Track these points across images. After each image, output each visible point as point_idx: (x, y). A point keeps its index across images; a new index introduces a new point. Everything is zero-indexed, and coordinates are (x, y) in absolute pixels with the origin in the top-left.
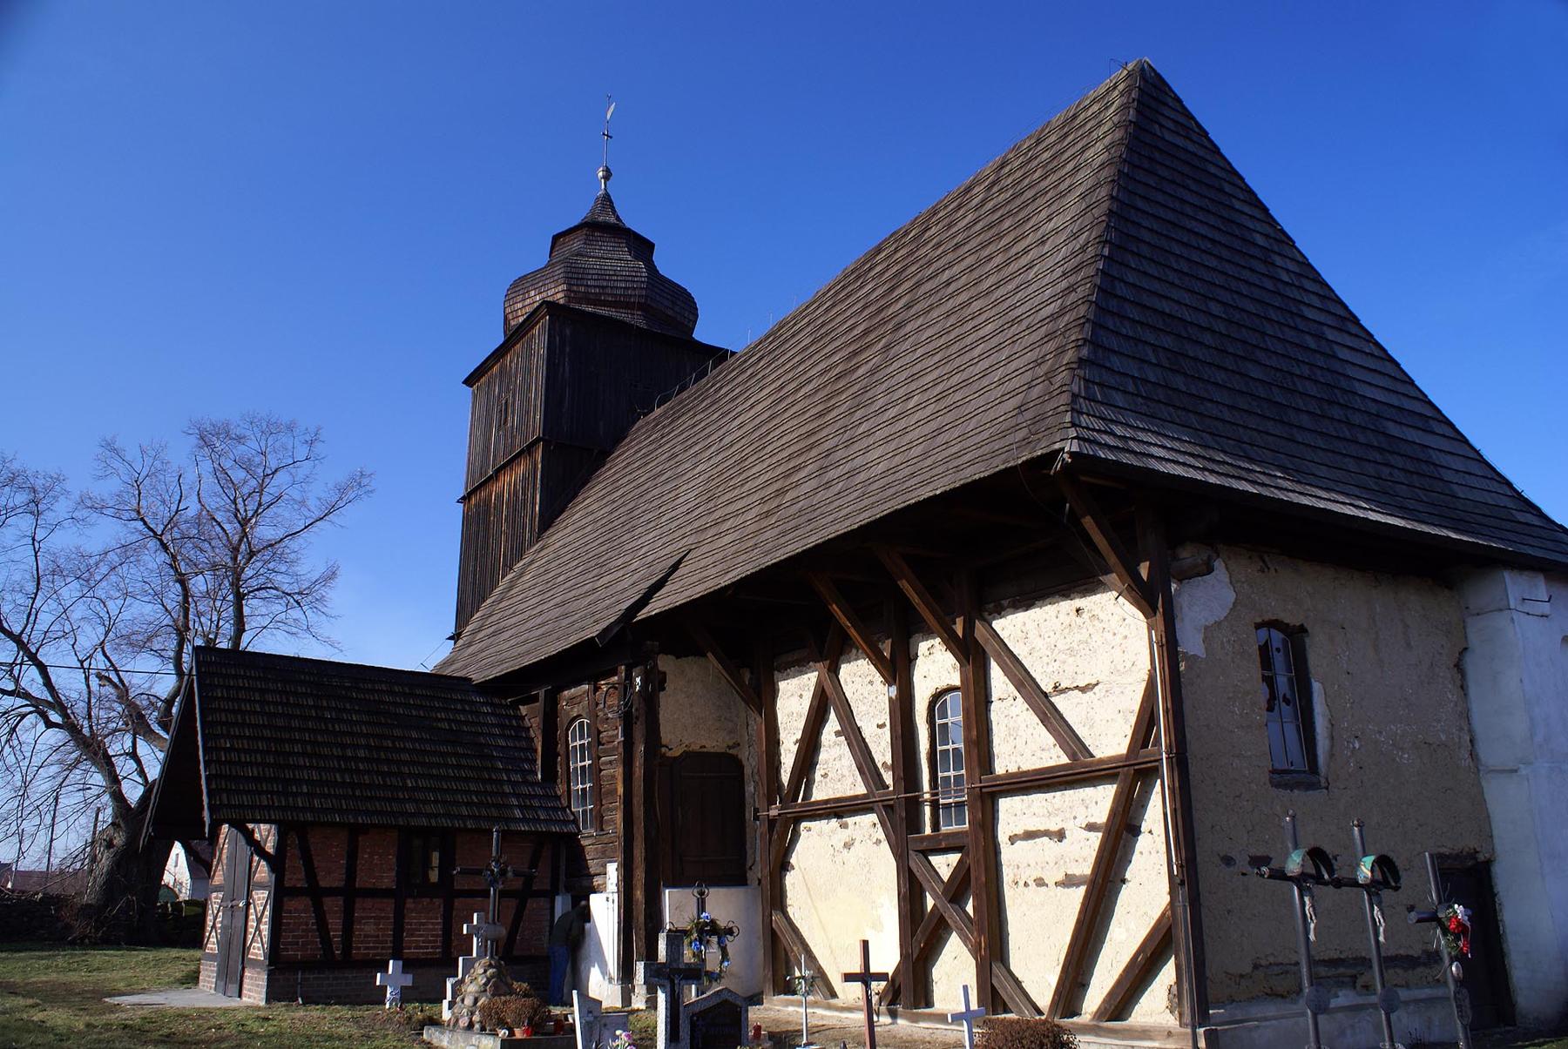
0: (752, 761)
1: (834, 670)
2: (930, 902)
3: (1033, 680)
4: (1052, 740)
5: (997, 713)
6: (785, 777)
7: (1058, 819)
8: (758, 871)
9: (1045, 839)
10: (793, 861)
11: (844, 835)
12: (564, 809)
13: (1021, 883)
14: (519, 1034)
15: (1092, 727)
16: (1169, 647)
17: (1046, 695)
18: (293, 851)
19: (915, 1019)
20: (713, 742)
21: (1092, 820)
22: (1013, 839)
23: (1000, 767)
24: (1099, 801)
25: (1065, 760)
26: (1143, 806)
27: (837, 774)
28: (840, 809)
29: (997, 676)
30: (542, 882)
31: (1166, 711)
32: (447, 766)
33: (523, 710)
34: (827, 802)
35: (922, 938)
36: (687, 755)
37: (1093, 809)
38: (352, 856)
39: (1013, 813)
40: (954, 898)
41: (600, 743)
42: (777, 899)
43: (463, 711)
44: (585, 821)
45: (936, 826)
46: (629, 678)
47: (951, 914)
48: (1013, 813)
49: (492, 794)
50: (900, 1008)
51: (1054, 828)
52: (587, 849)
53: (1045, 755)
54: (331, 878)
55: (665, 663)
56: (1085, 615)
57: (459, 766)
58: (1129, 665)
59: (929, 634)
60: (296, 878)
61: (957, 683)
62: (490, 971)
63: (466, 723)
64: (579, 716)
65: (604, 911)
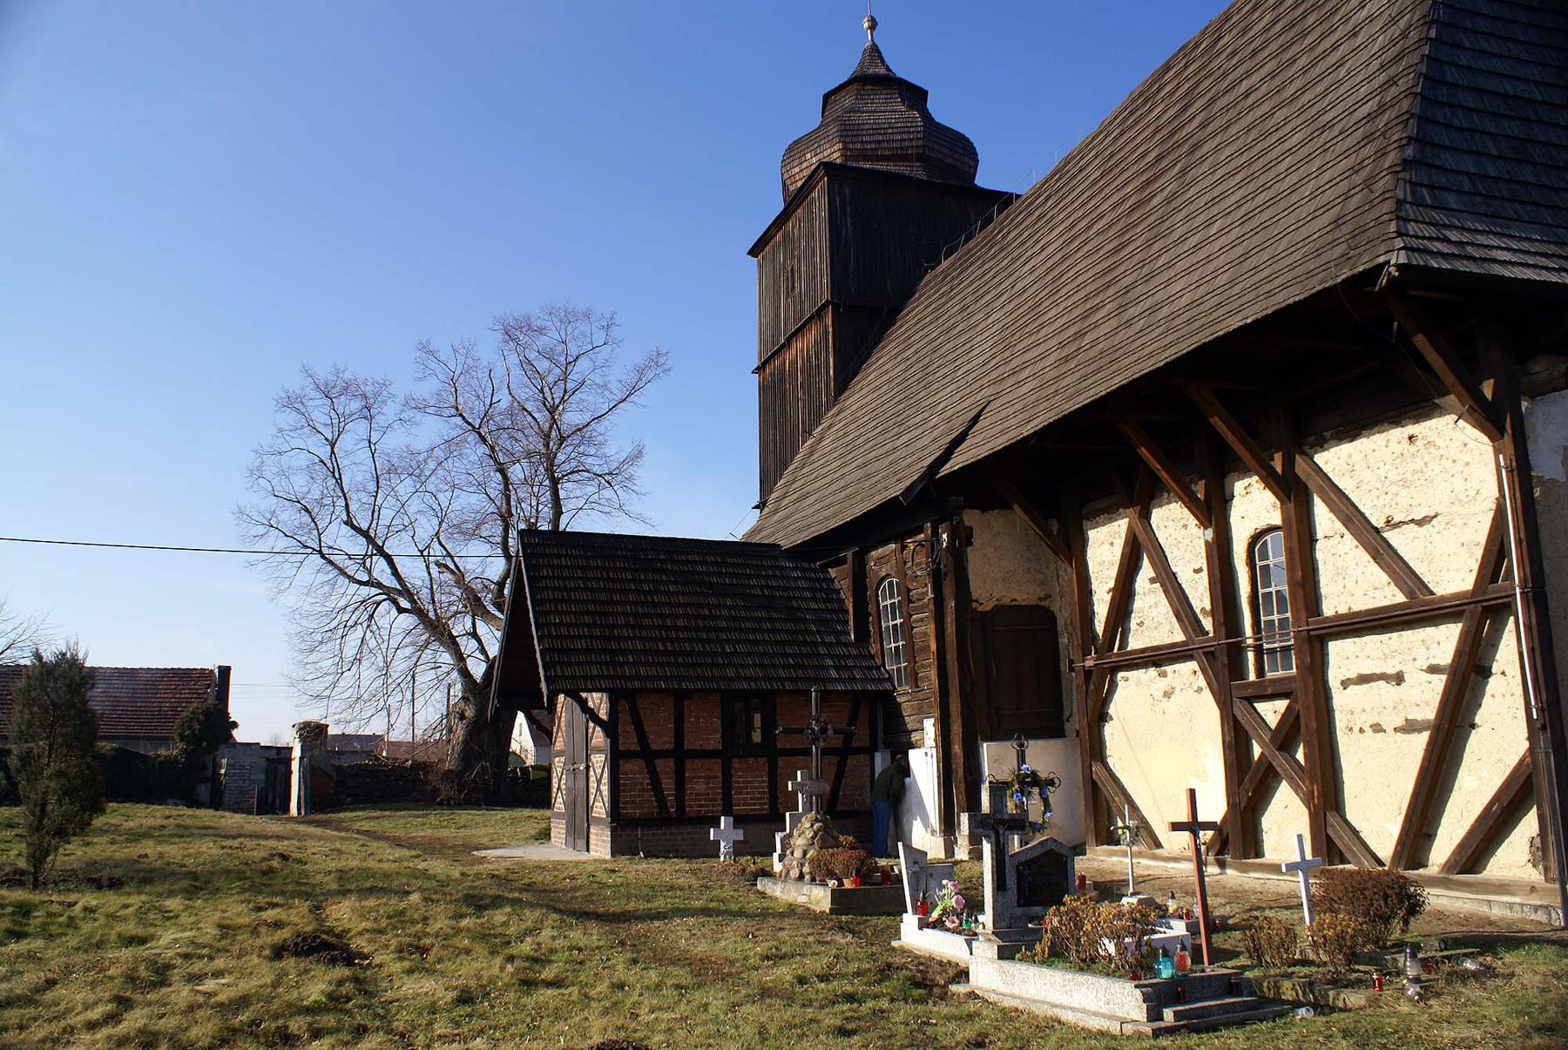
0: (1064, 613)
1: (1145, 516)
2: (1257, 751)
3: (1362, 515)
4: (1385, 578)
5: (1322, 552)
6: (1100, 627)
7: (1395, 661)
8: (1076, 721)
9: (1382, 683)
10: (1111, 711)
11: (1163, 684)
12: (878, 668)
13: (1356, 730)
14: (848, 884)
15: (1430, 563)
16: (1520, 471)
17: (1377, 530)
18: (624, 717)
19: (1245, 869)
20: (1024, 594)
21: (1435, 662)
22: (1345, 684)
23: (1328, 610)
24: (1443, 641)
25: (1401, 598)
26: (1493, 645)
27: (1153, 622)
28: (1157, 658)
29: (1322, 514)
30: (861, 740)
31: (1519, 542)
32: (762, 630)
33: (833, 572)
34: (1144, 650)
35: (1250, 786)
36: (999, 609)
37: (1434, 650)
38: (679, 719)
39: (1344, 657)
40: (1285, 745)
41: (910, 601)
42: (1095, 750)
43: (775, 576)
44: (899, 679)
45: (1260, 671)
46: (936, 534)
47: (1280, 762)
48: (1344, 657)
49: (807, 656)
50: (1228, 858)
51: (1391, 671)
52: (904, 706)
53: (1378, 594)
54: (661, 740)
55: (971, 518)
56: (1420, 443)
57: (774, 631)
58: (1472, 493)
59: (1245, 472)
60: (630, 742)
61: (1278, 521)
62: (817, 825)
63: (778, 588)
64: (888, 576)
65: (924, 766)
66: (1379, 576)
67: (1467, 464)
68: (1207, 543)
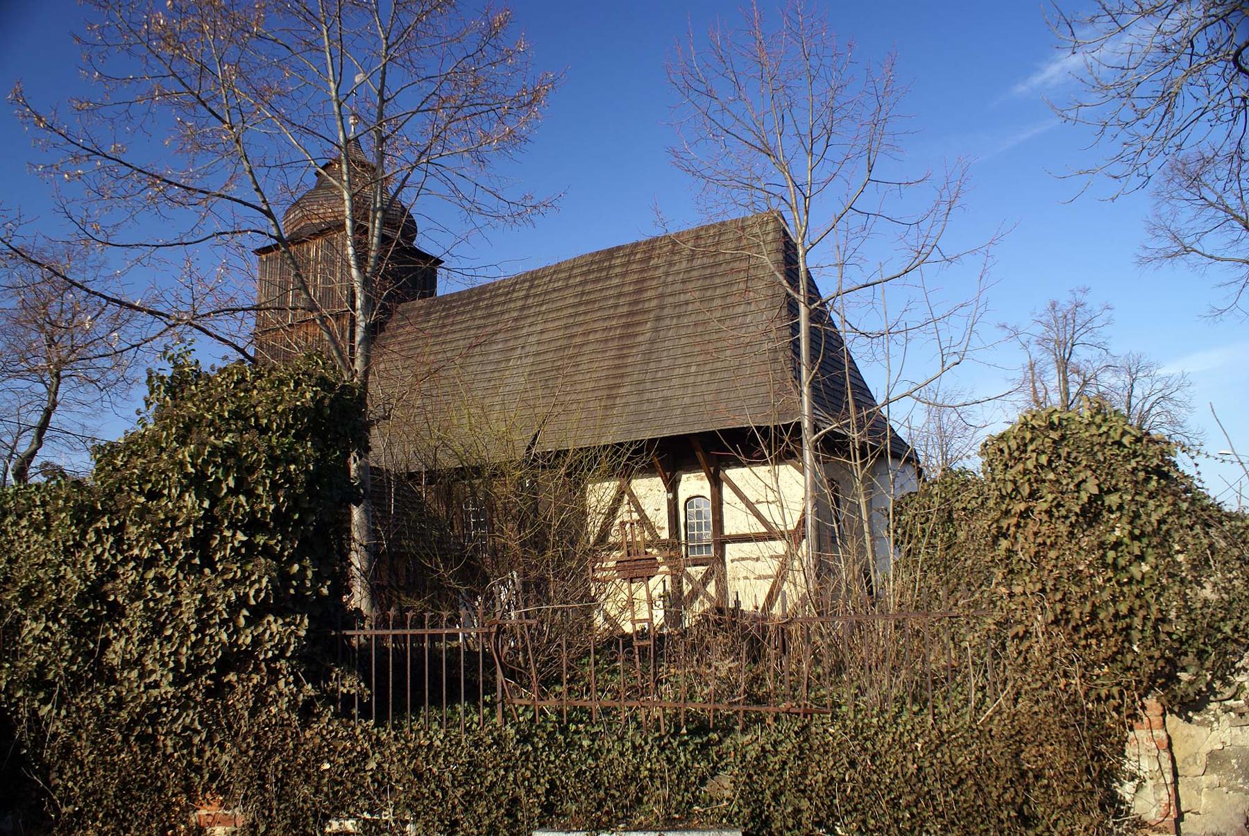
5: (726, 509)
22: (732, 561)
23: (727, 532)
29: (727, 492)
39: (731, 550)
48: (731, 550)
66: (753, 520)
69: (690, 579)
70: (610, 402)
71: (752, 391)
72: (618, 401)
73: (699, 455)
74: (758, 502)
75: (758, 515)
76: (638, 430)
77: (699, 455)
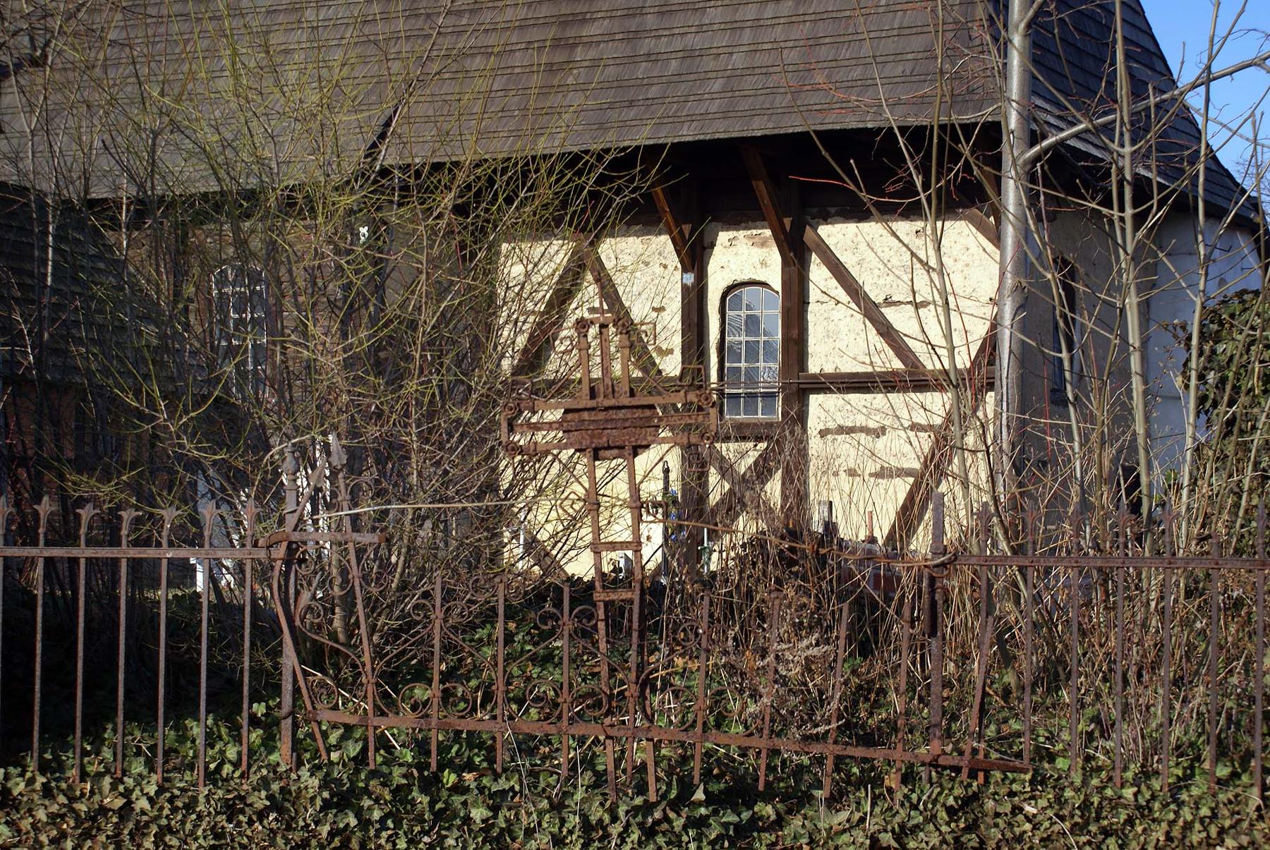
17: (876, 306)
22: (823, 433)
23: (814, 367)
39: (821, 409)
48: (821, 409)
67: (967, 265)
68: (684, 287)
69: (726, 470)
70: (560, 57)
71: (889, 46)
72: (579, 54)
73: (761, 187)
74: (888, 302)
75: (887, 332)
76: (624, 125)
77: (761, 187)
